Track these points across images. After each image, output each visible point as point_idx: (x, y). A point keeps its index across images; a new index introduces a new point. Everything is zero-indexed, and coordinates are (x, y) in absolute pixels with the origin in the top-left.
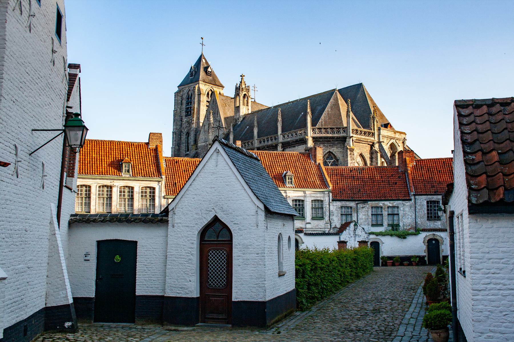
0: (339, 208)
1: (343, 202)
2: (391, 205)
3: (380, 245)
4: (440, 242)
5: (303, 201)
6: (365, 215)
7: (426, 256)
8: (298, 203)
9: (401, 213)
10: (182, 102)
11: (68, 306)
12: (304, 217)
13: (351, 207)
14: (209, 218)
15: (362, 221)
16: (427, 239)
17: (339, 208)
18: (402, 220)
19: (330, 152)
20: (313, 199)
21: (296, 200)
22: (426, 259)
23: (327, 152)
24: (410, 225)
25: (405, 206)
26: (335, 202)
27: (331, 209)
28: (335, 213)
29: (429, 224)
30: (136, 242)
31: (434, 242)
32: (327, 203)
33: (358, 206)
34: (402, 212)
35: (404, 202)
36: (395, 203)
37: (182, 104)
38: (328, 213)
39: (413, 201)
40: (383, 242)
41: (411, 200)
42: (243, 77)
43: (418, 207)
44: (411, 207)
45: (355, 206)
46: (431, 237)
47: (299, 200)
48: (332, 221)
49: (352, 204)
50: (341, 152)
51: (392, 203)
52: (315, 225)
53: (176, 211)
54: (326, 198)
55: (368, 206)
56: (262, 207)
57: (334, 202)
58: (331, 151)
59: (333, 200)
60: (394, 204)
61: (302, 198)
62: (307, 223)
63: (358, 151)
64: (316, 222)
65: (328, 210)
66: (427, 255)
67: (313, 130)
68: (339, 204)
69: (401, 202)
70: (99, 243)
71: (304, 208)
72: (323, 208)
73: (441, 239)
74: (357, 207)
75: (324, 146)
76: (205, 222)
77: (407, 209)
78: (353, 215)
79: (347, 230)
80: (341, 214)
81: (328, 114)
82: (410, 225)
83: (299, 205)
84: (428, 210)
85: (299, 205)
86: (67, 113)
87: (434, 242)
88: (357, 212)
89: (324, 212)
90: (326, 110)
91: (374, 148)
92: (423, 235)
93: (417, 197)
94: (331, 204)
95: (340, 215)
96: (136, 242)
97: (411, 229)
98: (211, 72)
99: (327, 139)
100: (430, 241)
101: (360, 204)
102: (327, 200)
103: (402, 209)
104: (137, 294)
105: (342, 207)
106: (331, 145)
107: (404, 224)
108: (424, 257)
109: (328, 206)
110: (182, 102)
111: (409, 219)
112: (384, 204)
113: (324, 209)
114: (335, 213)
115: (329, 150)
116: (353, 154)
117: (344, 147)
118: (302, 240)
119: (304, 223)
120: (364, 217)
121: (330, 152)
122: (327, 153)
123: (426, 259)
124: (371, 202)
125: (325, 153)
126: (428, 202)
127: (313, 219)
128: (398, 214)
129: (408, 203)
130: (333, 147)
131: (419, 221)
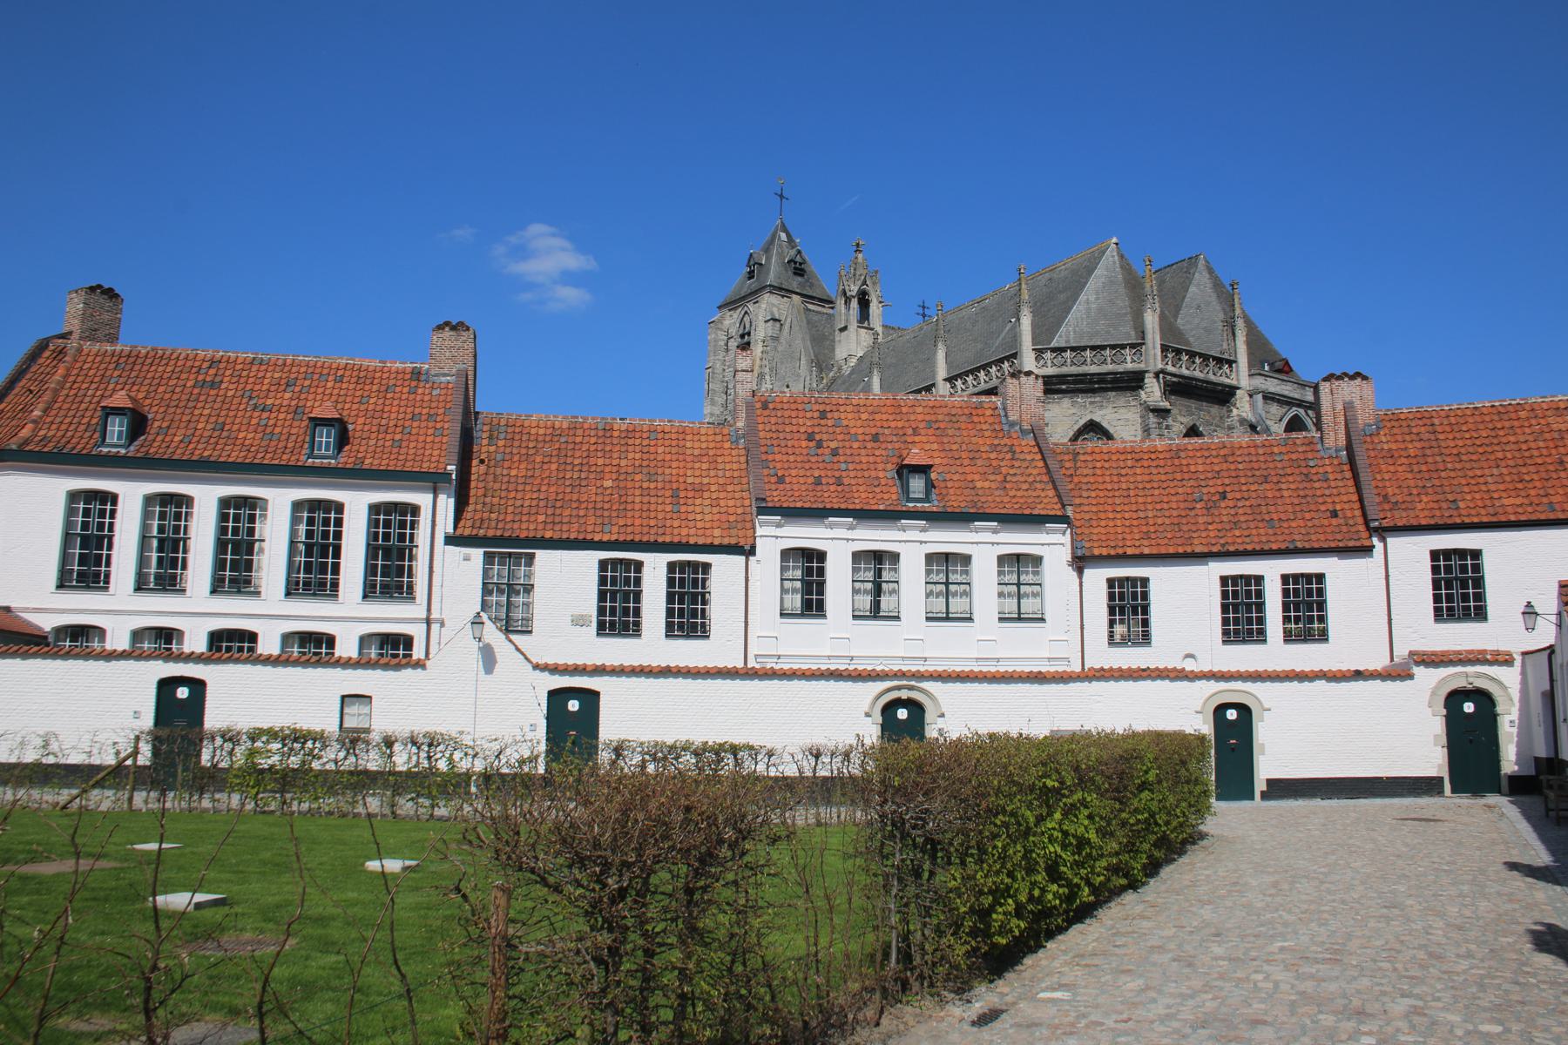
19: (1093, 428)
23: (1082, 422)
31: (1469, 707)
46: (1460, 683)
50: (1128, 420)
58: (1097, 419)
67: (1039, 353)
81: (1088, 310)
90: (1082, 297)
91: (1235, 412)
92: (1430, 680)
98: (800, 264)
99: (1081, 382)
100: (1455, 698)
115: (1088, 418)
116: (1168, 427)
125: (1076, 427)
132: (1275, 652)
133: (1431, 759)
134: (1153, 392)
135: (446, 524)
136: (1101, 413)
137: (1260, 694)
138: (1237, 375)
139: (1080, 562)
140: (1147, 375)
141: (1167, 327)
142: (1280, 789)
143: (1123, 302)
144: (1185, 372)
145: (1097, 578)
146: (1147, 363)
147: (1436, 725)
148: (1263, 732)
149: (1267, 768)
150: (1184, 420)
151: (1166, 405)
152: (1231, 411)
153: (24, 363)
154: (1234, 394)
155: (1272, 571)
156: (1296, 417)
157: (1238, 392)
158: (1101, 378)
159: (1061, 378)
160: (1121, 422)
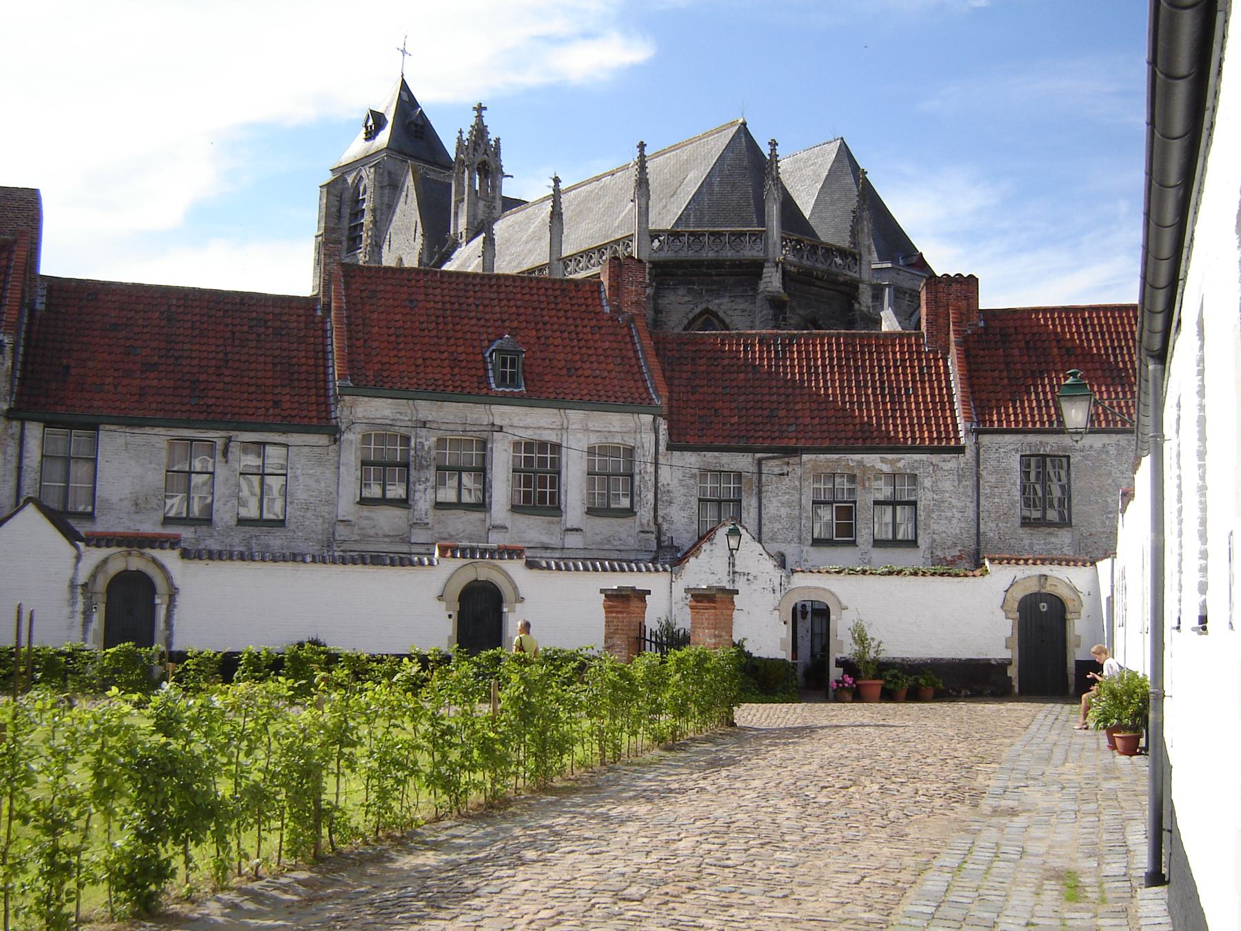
0: (693, 476)
1: (709, 454)
2: (886, 468)
3: (832, 617)
4: (1070, 606)
5: (557, 448)
6: (788, 504)
7: (1010, 662)
8: (536, 455)
9: (925, 499)
10: (339, 211)
12: (559, 508)
13: (739, 475)
15: (777, 526)
16: (1019, 594)
17: (693, 476)
18: (927, 526)
20: (594, 440)
21: (529, 446)
22: (1013, 672)
23: (697, 311)
24: (955, 545)
25: (939, 473)
26: (679, 453)
27: (662, 480)
28: (678, 493)
29: (1027, 542)
32: (650, 458)
33: (765, 469)
34: (929, 495)
35: (935, 458)
36: (905, 461)
37: (339, 217)
38: (651, 496)
39: (969, 453)
40: (844, 603)
41: (960, 450)
42: (484, 113)
43: (988, 478)
44: (960, 478)
45: (753, 469)
46: (1033, 588)
47: (543, 445)
48: (665, 526)
49: (742, 462)
50: (743, 311)
51: (892, 462)
52: (598, 538)
55: (799, 471)
57: (677, 454)
58: (715, 308)
59: (671, 448)
60: (900, 464)
61: (552, 437)
62: (568, 530)
63: (802, 312)
64: (603, 526)
65: (651, 484)
66: (1016, 657)
68: (692, 459)
69: (924, 457)
71: (559, 473)
72: (632, 476)
73: (1073, 596)
74: (760, 473)
75: (690, 291)
77: (947, 485)
78: (744, 504)
79: (702, 555)
80: (700, 500)
82: (955, 545)
83: (543, 461)
84: (1024, 490)
85: (543, 461)
87: (1044, 607)
88: (760, 492)
89: (636, 489)
91: (856, 306)
93: (985, 439)
94: (661, 460)
95: (694, 502)
97: (960, 557)
101: (772, 463)
102: (646, 446)
103: (927, 483)
105: (704, 472)
106: (714, 287)
107: (934, 541)
108: (1003, 665)
109: (651, 469)
110: (339, 211)
111: (955, 521)
112: (860, 463)
113: (637, 478)
114: (678, 493)
115: (704, 306)
117: (754, 296)
118: (515, 588)
119: (557, 529)
120: (784, 511)
121: (707, 311)
122: (701, 314)
123: (1013, 672)
124: (813, 456)
125: (691, 316)
126: (1025, 460)
127: (591, 511)
128: (914, 504)
129: (950, 463)
130: (718, 297)
131: (988, 528)
134: (772, 281)
136: (717, 301)
138: (860, 269)
140: (766, 265)
144: (805, 262)
146: (766, 249)
150: (802, 312)
151: (786, 297)
152: (853, 305)
154: (857, 288)
157: (861, 285)
158: (717, 264)
159: (679, 264)
160: (738, 312)
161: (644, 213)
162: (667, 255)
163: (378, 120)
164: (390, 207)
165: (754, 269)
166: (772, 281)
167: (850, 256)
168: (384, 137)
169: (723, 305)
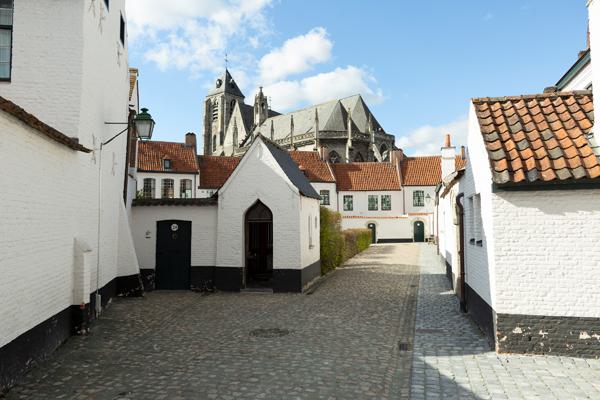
11: (136, 275)
14: (253, 201)
30: (190, 222)
53: (224, 195)
54: (332, 187)
56: (297, 190)
70: (159, 223)
76: (250, 204)
86: (130, 110)
96: (190, 222)
100: (416, 223)
104: (193, 264)
121: (333, 151)
132: (380, 212)
133: (411, 235)
134: (349, 143)
135: (198, 184)
137: (377, 221)
139: (338, 190)
141: (353, 125)
142: (381, 241)
143: (341, 119)
145: (342, 194)
147: (412, 228)
148: (378, 229)
149: (378, 237)
153: (38, 130)
155: (379, 195)
156: (384, 145)
161: (317, 127)
162: (323, 137)
163: (220, 81)
164: (230, 111)
165: (346, 140)
166: (349, 143)
167: (367, 135)
168: (223, 87)
169: (338, 149)
